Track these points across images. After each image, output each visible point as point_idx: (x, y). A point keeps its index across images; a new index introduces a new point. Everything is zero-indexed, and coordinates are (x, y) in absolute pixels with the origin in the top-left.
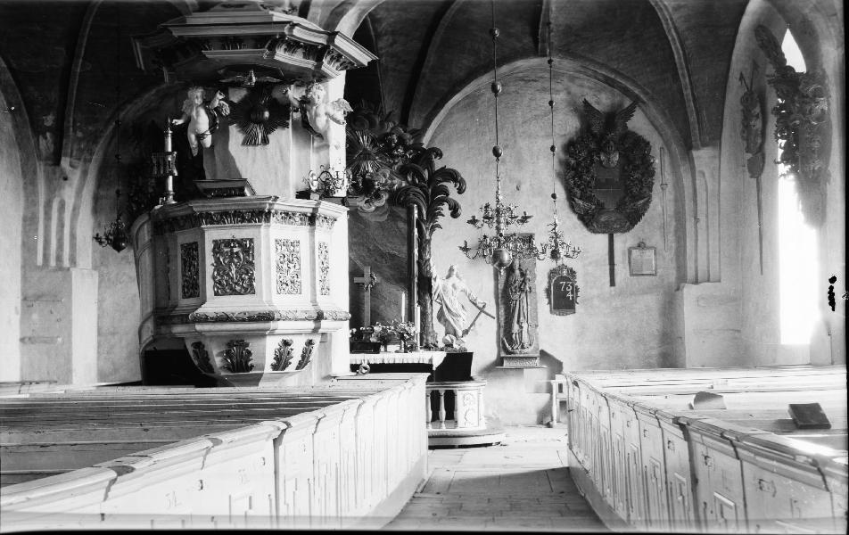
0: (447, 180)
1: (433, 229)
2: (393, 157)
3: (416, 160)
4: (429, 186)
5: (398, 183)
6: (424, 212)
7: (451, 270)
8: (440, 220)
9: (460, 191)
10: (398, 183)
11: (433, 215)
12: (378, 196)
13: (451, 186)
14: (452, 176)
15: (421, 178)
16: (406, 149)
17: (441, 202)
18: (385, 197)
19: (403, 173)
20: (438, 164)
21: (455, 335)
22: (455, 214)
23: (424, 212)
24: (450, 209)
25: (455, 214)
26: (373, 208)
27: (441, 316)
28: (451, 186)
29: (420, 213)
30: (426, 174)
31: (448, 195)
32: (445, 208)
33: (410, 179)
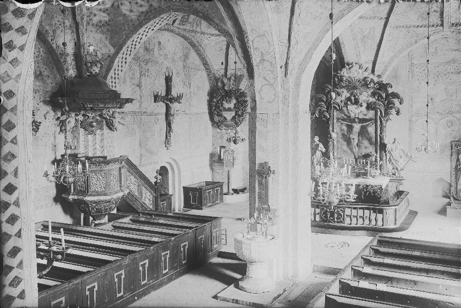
0: (393, 98)
1: (387, 120)
2: (368, 88)
4: (385, 101)
5: (372, 100)
6: (383, 113)
7: (395, 139)
8: (391, 116)
10: (372, 100)
11: (387, 114)
13: (396, 101)
14: (395, 95)
15: (382, 97)
17: (391, 108)
18: (365, 105)
19: (373, 94)
20: (390, 90)
21: (397, 169)
22: (398, 113)
23: (383, 113)
25: (398, 113)
27: (390, 160)
28: (396, 101)
29: (381, 113)
30: (384, 95)
31: (394, 105)
32: (393, 111)
33: (376, 98)
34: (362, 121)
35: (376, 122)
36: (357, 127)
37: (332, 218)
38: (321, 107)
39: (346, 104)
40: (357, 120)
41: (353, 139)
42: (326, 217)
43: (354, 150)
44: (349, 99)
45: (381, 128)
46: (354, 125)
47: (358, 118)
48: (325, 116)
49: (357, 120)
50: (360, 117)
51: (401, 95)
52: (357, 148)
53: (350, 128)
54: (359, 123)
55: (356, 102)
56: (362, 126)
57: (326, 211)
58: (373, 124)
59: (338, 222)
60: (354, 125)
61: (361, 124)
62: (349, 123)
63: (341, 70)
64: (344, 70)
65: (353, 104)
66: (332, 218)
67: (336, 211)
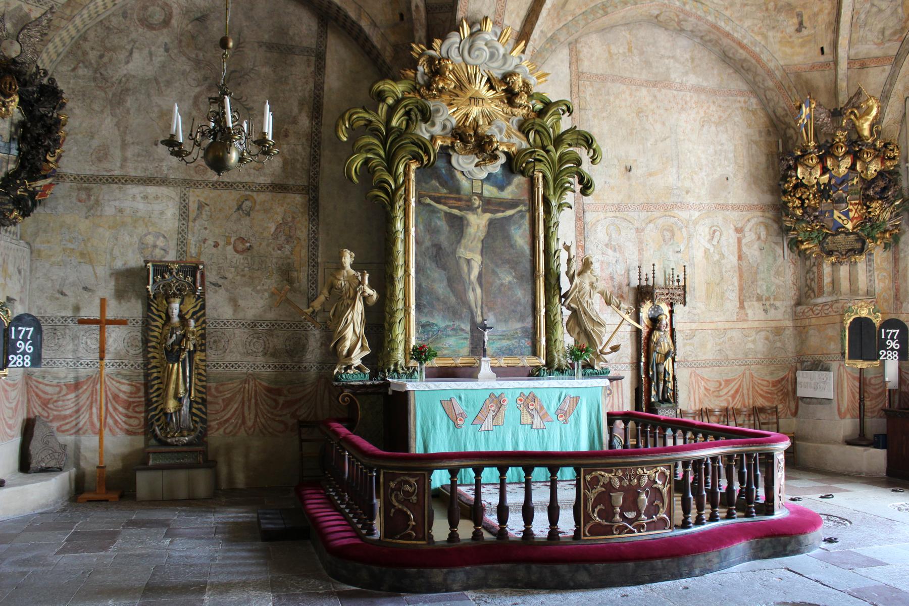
1: (560, 206)
3: (541, 113)
9: (593, 161)
12: (495, 158)
13: (583, 154)
16: (530, 96)
18: (503, 159)
20: (565, 123)
24: (580, 182)
26: (484, 175)
34: (489, 204)
35: (533, 210)
36: (478, 223)
37: (631, 515)
38: (369, 151)
39: (446, 153)
40: (477, 202)
41: (468, 261)
42: (607, 514)
43: (471, 296)
44: (459, 134)
45: (547, 229)
46: (472, 218)
47: (480, 196)
48: (381, 185)
49: (477, 202)
50: (486, 194)
51: (598, 143)
52: (479, 291)
53: (458, 225)
54: (484, 211)
55: (482, 146)
56: (491, 223)
57: (609, 486)
58: (523, 217)
59: (652, 526)
60: (472, 218)
61: (488, 216)
62: (456, 212)
63: (443, 38)
64: (454, 38)
65: (471, 152)
66: (631, 515)
67: (645, 480)
